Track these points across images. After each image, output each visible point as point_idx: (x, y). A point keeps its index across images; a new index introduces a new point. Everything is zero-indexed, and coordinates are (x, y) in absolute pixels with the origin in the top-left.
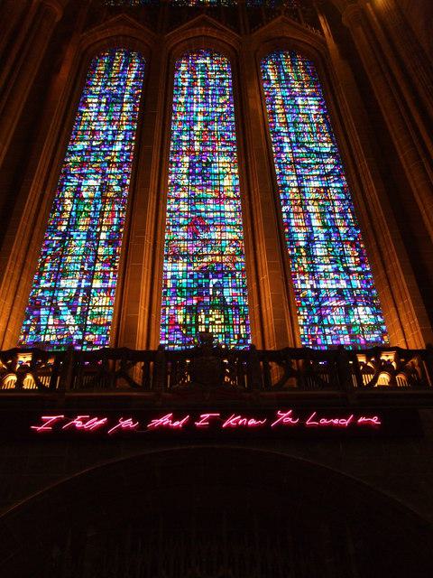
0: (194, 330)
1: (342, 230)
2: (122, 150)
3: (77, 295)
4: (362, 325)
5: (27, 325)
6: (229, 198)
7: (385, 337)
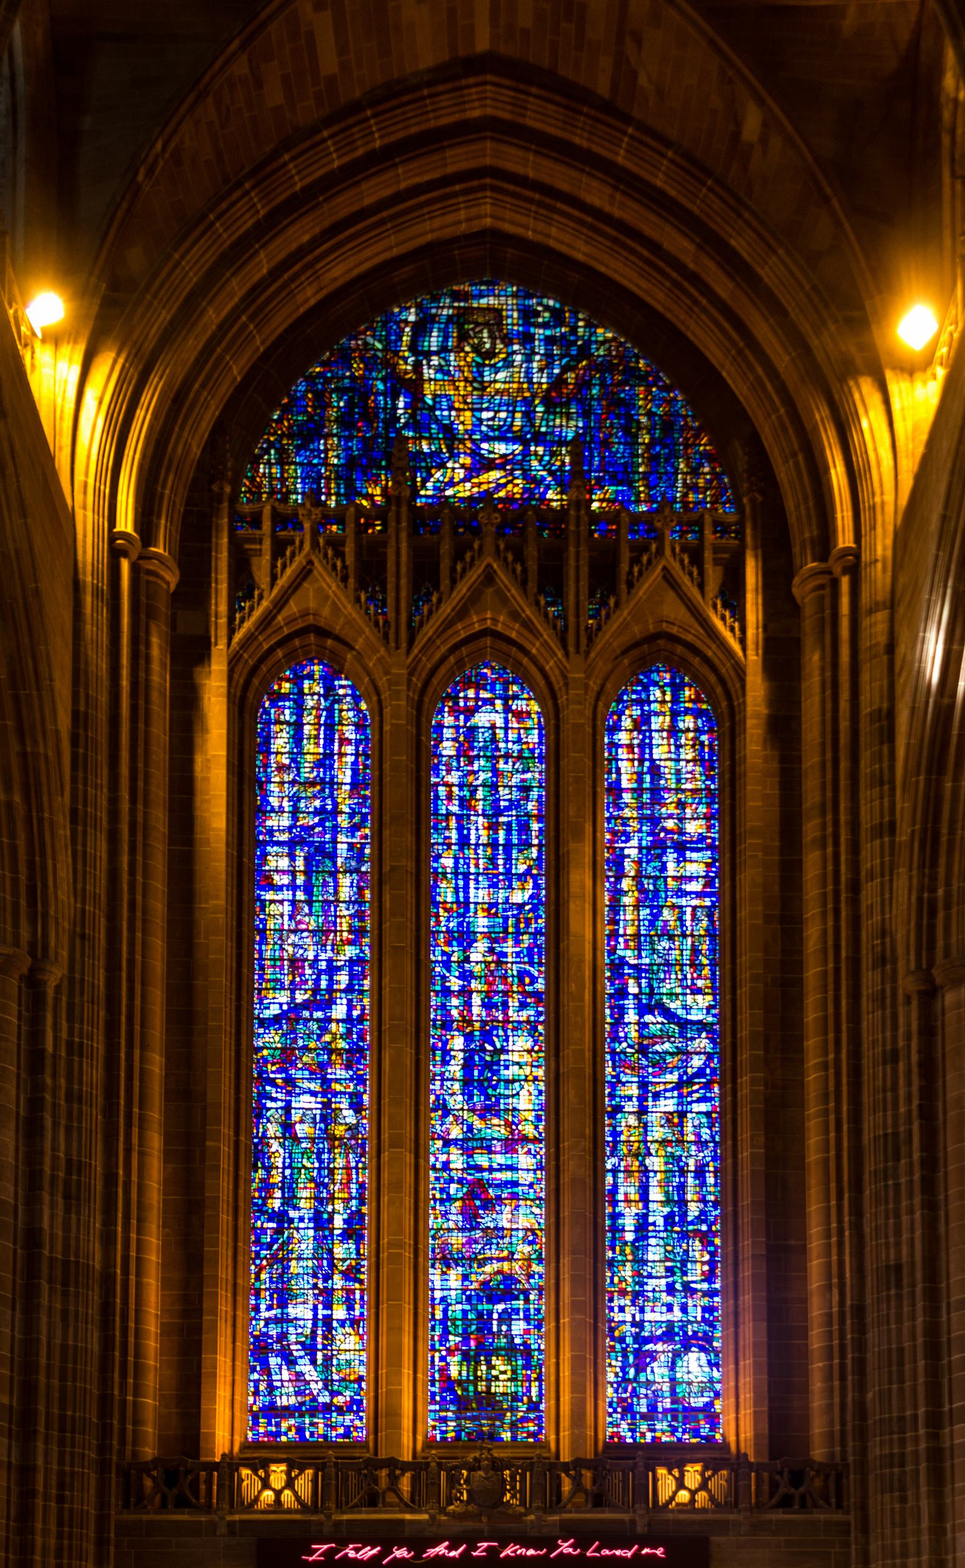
0: (471, 1388)
1: (693, 1210)
2: (349, 1020)
3: (314, 1332)
4: (689, 1383)
5: (255, 1381)
6: (525, 1139)
7: (716, 1402)
